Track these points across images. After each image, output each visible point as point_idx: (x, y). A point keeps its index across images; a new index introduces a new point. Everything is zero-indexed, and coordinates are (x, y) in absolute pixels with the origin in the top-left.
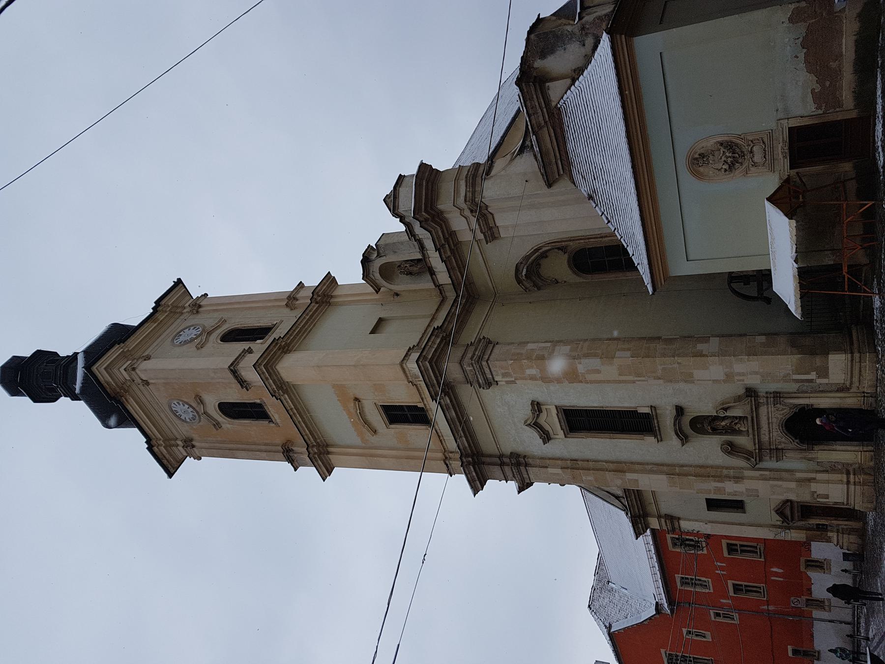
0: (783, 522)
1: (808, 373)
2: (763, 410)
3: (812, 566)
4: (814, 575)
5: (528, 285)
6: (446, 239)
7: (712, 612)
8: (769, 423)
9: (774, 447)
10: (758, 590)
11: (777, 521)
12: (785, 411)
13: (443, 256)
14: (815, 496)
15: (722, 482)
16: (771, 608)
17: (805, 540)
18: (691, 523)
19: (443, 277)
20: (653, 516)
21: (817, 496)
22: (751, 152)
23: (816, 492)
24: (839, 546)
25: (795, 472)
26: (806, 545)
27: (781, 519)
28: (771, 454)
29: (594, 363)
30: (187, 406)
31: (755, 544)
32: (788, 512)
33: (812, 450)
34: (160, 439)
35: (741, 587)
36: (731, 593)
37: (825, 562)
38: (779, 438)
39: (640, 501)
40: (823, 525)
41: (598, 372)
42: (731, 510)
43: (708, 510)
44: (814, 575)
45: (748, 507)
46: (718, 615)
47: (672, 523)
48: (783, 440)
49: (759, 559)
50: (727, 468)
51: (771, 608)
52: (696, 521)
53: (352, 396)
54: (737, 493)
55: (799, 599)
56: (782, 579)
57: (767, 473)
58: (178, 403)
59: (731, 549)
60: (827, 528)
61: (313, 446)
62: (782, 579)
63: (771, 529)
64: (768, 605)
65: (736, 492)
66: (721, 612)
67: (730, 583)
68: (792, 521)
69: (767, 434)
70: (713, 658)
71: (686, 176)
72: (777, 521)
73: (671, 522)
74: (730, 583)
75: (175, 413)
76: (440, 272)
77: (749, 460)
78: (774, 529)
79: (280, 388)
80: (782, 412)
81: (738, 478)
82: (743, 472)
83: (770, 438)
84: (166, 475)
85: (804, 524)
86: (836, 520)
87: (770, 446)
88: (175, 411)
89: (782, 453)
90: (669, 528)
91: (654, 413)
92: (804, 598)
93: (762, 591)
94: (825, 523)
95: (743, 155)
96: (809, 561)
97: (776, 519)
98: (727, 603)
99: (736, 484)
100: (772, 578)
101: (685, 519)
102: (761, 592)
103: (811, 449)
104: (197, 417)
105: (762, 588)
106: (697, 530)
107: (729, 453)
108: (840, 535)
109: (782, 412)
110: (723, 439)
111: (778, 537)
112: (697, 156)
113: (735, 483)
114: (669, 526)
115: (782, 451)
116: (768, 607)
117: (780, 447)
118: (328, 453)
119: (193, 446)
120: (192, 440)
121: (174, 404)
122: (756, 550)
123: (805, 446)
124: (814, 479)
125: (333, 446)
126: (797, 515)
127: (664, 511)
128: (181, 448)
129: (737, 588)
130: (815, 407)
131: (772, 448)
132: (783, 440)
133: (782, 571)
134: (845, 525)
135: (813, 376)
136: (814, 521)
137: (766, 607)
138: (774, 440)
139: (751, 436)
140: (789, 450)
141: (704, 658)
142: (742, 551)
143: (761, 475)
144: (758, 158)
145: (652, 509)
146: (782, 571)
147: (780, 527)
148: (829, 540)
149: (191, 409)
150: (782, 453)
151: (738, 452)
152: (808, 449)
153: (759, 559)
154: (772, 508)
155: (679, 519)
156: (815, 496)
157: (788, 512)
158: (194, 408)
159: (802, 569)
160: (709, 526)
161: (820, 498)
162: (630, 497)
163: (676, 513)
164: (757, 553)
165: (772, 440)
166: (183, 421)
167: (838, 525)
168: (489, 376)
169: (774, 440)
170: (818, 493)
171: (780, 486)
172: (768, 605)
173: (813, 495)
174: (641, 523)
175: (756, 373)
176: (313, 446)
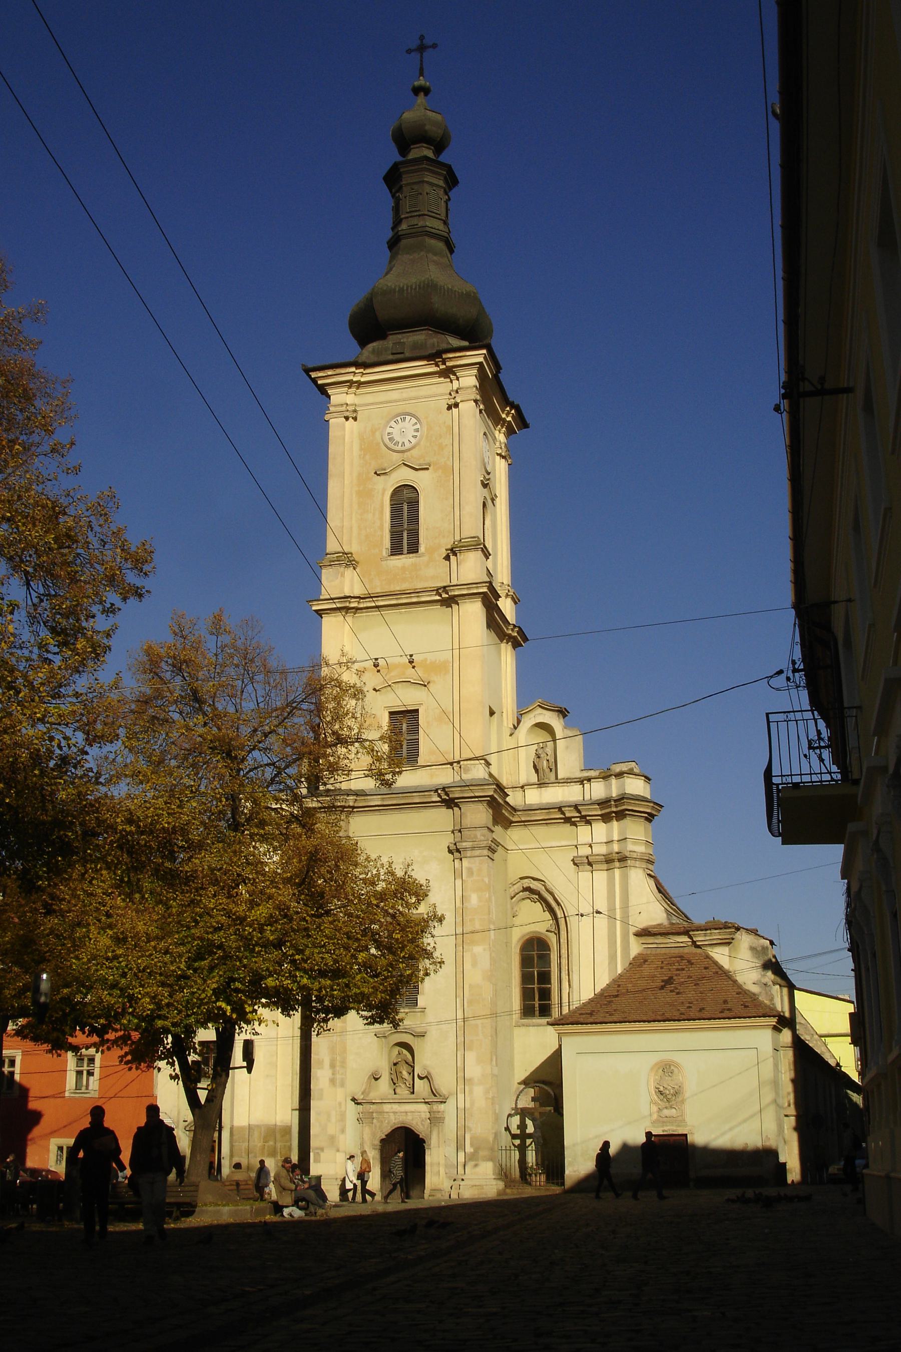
1: (472, 1145)
2: (424, 1108)
5: (515, 887)
6: (585, 817)
8: (406, 1112)
12: (421, 1127)
13: (567, 809)
14: (317, 1151)
15: (333, 1066)
19: (534, 797)
22: (671, 1107)
29: (485, 962)
30: (413, 441)
41: (474, 964)
48: (385, 1124)
53: (432, 679)
58: (417, 430)
71: (655, 1058)
76: (541, 794)
80: (419, 1124)
84: (311, 366)
91: (417, 1010)
95: (668, 1101)
104: (391, 446)
109: (419, 1124)
112: (672, 1067)
119: (347, 418)
120: (355, 419)
123: (377, 1142)
130: (427, 1152)
135: (469, 1149)
139: (390, 1097)
144: (666, 1112)
149: (408, 445)
158: (409, 450)
166: (388, 422)
168: (469, 853)
170: (322, 1154)
173: (317, 1148)
175: (472, 1103)
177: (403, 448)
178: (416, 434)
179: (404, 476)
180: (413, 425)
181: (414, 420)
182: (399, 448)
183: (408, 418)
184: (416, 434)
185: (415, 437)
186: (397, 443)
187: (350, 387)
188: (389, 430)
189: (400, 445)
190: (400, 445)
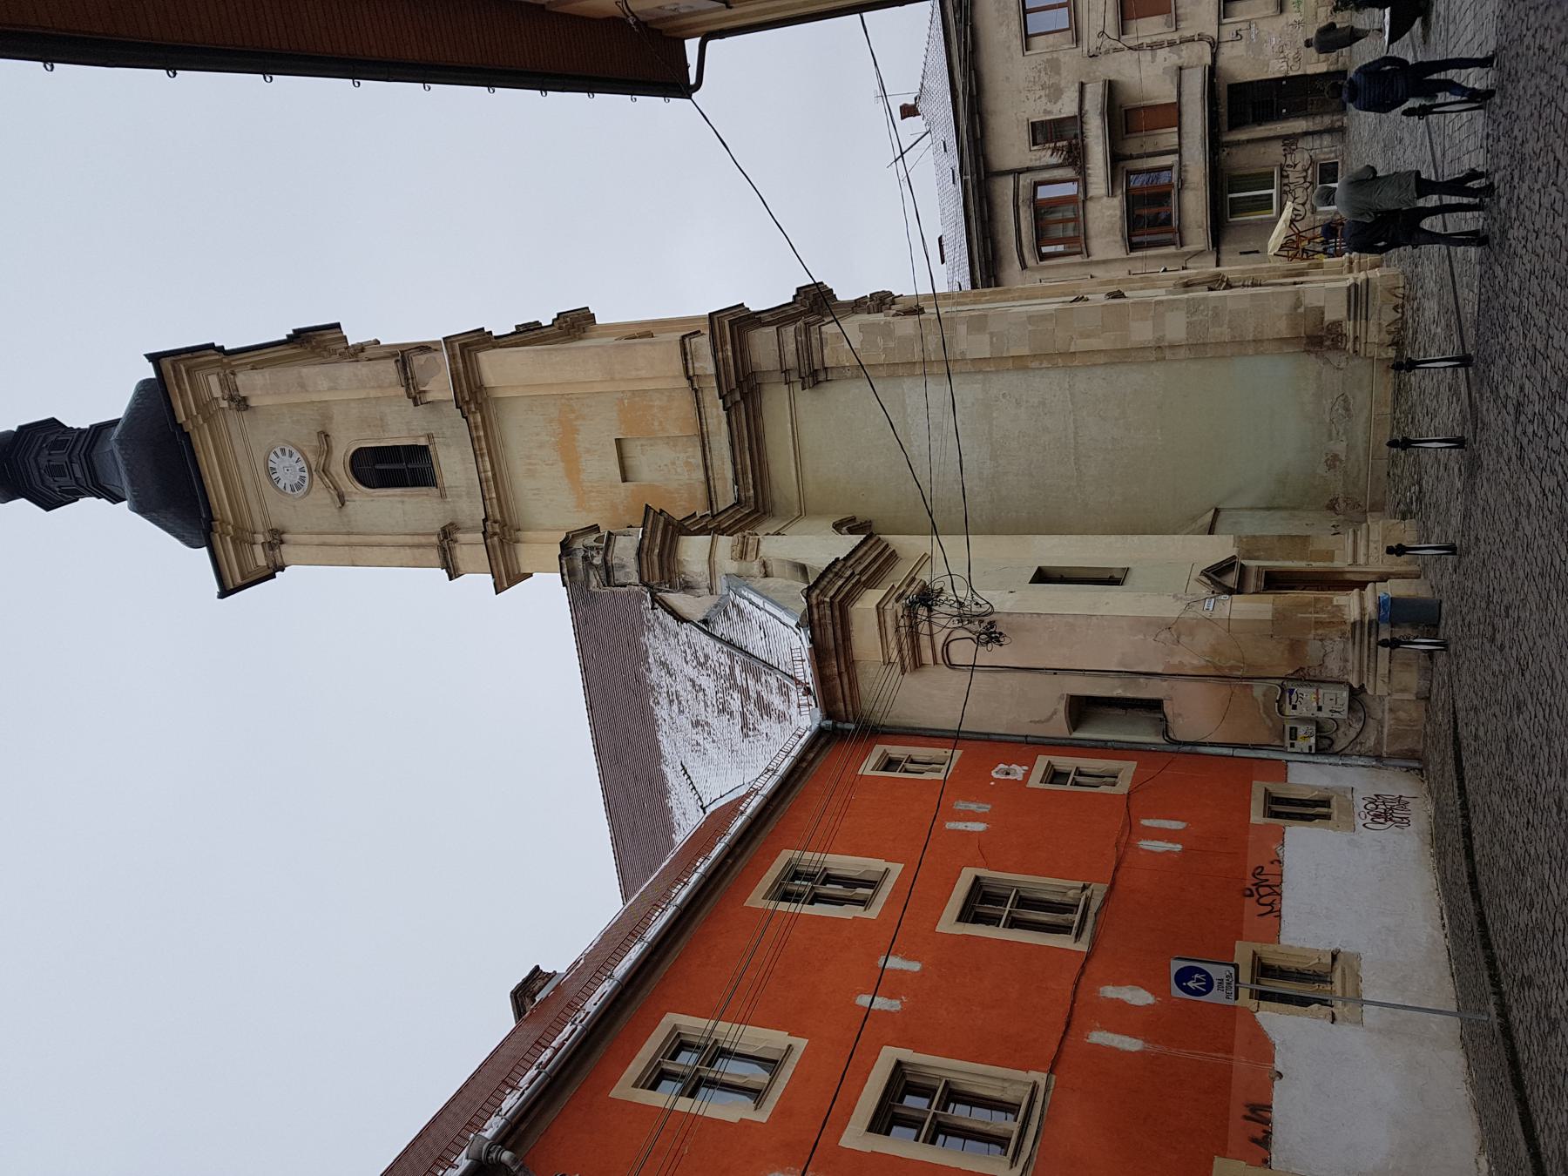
30: (297, 455)
34: (229, 524)
58: (283, 450)
61: (495, 522)
75: (270, 471)
79: (473, 394)
88: (273, 469)
118: (518, 541)
121: (275, 453)
125: (529, 530)
128: (258, 550)
149: (303, 464)
176: (495, 522)
177: (306, 469)
178: (287, 452)
179: (340, 466)
180: (278, 457)
181: (272, 456)
182: (306, 474)
183: (271, 465)
184: (287, 452)
185: (291, 455)
186: (302, 478)
187: (243, 541)
188: (288, 490)
189: (303, 474)
190: (303, 474)
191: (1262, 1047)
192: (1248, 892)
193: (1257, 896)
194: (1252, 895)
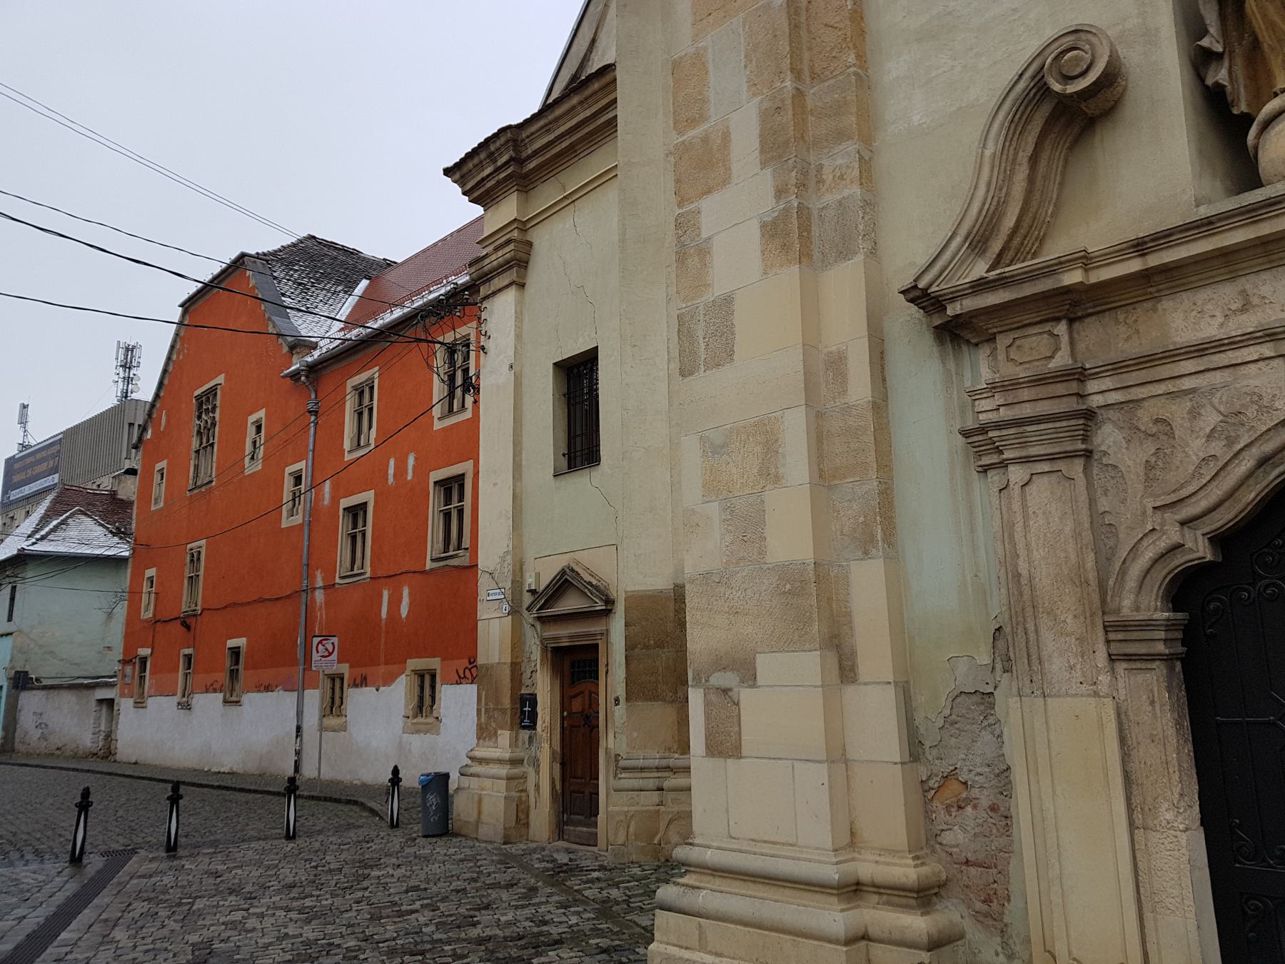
0: (533, 592)
3: (422, 688)
4: (399, 692)
7: (301, 465)
9: (1096, 401)
10: (358, 562)
11: (538, 575)
16: (319, 596)
17: (481, 660)
18: (512, 323)
20: (522, 206)
21: (726, 691)
23: (749, 676)
24: (469, 762)
25: (887, 558)
26: (471, 672)
27: (542, 588)
28: (1040, 381)
31: (466, 543)
32: (570, 603)
33: (1112, 658)
35: (360, 523)
36: (345, 503)
37: (431, 720)
38: (1211, 419)
39: (571, 147)
40: (533, 716)
42: (563, 436)
43: (554, 364)
44: (399, 692)
45: (582, 481)
46: (298, 479)
47: (505, 267)
49: (428, 558)
50: (866, 168)
51: (319, 596)
52: (518, 337)
54: (693, 262)
55: (334, 656)
56: (384, 614)
57: (860, 388)
59: (453, 487)
60: (524, 728)
62: (384, 614)
63: (509, 559)
64: (325, 588)
65: (704, 252)
66: (303, 486)
67: (368, 496)
68: (539, 618)
69: (1249, 322)
70: (214, 483)
72: (538, 575)
73: (508, 262)
74: (368, 496)
77: (978, 243)
78: (508, 569)
81: (805, 228)
82: (844, 254)
83: (1201, 350)
85: (533, 658)
86: (553, 753)
87: (1117, 368)
89: (1051, 458)
90: (487, 261)
92: (345, 669)
93: (356, 571)
94: (539, 723)
96: (433, 677)
97: (541, 573)
98: (323, 495)
99: (757, 233)
100: (386, 594)
101: (520, 304)
102: (352, 570)
103: (1115, 648)
105: (362, 571)
106: (490, 345)
107: (1039, 90)
108: (504, 771)
110: (1132, 58)
111: (484, 583)
113: (763, 226)
114: (493, 257)
115: (1069, 456)
116: (320, 588)
117: (1108, 437)
122: (451, 548)
124: (847, 671)
126: (564, 633)
127: (545, 240)
129: (356, 512)
131: (1092, 386)
132: (1196, 448)
133: (404, 616)
134: (537, 787)
136: (544, 689)
137: (319, 583)
138: (1187, 384)
140: (1092, 502)
141: (214, 465)
142: (447, 515)
143: (837, 364)
145: (547, 194)
146: (404, 616)
147: (517, 583)
148: (484, 732)
150: (1051, 458)
151: (1034, 160)
152: (1124, 626)
153: (428, 558)
154: (578, 556)
155: (522, 286)
156: (718, 679)
157: (570, 603)
159: (414, 664)
160: (506, 377)
161: (707, 704)
162: (581, 103)
163: (539, 273)
164: (445, 552)
165: (1189, 366)
167: (536, 763)
169: (1187, 384)
170: (746, 696)
171: (770, 474)
172: (325, 588)
173: (721, 665)
174: (497, 170)
191: (389, 680)
192: (472, 660)
193: (470, 666)
194: (470, 663)
